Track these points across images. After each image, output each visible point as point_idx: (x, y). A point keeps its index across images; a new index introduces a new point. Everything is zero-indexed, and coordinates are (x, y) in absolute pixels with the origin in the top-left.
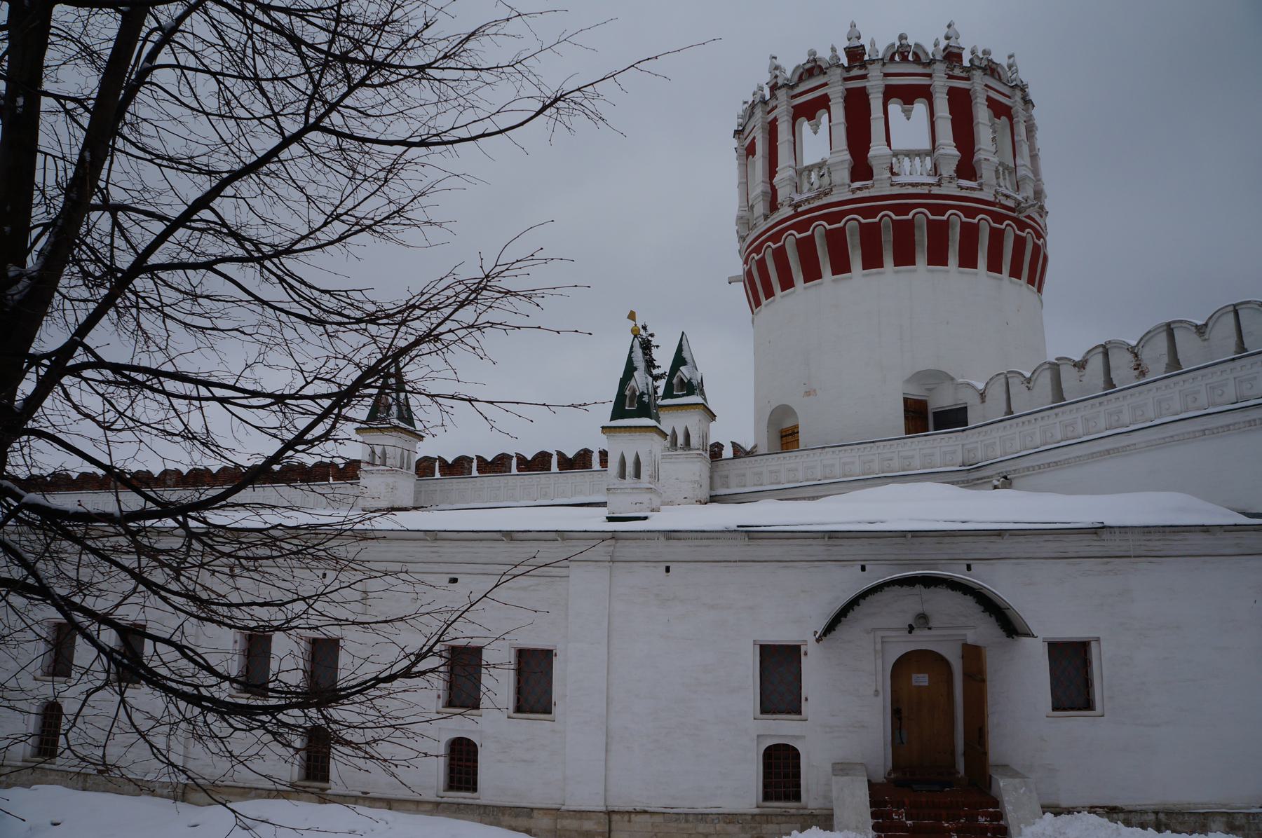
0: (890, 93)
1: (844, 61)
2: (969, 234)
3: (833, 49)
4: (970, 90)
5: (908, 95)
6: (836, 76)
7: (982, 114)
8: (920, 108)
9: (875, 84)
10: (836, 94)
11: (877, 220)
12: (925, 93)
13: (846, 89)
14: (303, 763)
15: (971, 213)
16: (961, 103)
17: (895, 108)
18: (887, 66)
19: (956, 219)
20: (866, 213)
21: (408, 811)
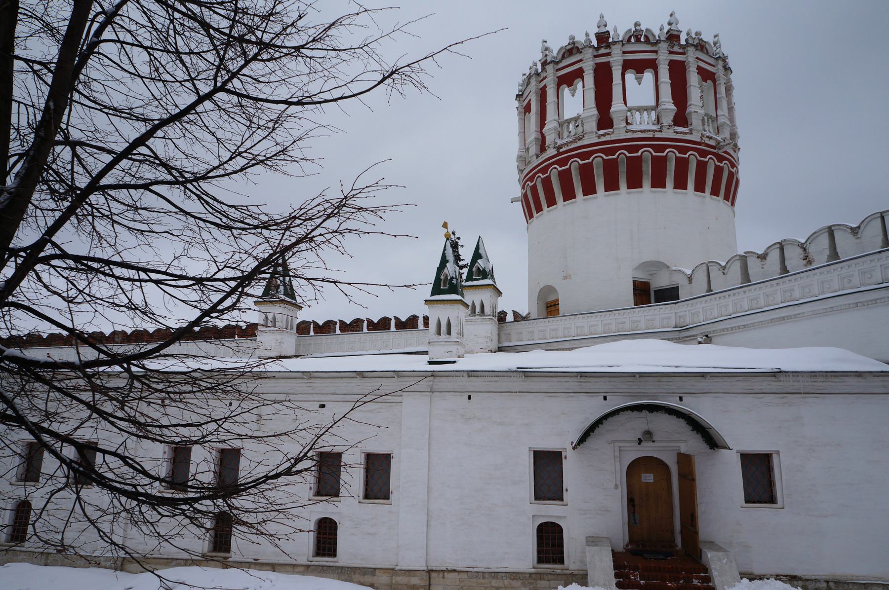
1: (595, 43)
2: (682, 166)
3: (587, 35)
5: (639, 67)
6: (588, 54)
9: (616, 59)
12: (652, 65)
13: (595, 64)
14: (212, 539)
18: (626, 46)
19: (672, 155)
21: (287, 572)
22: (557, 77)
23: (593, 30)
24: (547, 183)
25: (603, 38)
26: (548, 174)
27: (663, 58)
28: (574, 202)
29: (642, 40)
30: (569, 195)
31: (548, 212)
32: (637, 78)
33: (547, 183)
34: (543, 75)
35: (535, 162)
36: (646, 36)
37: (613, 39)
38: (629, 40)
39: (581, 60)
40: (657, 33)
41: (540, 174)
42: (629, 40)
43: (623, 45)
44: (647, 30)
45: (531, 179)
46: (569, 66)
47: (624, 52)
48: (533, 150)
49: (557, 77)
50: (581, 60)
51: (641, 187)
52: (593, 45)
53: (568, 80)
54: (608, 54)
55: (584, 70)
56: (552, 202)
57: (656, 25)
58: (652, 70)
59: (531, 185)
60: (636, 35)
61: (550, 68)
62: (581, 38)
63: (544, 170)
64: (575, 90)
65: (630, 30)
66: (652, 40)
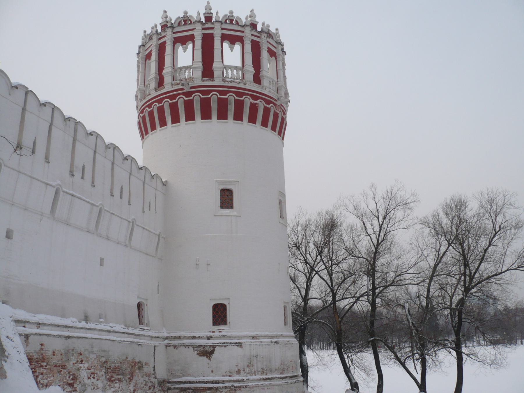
0: (224, 38)
1: (203, 20)
2: (254, 109)
3: (199, 14)
4: (260, 42)
6: (199, 27)
7: (265, 54)
8: (237, 47)
9: (217, 33)
10: (198, 34)
11: (209, 96)
12: (240, 40)
15: (255, 98)
16: (256, 47)
17: (226, 45)
18: (223, 24)
19: (248, 101)
20: (203, 92)
22: (174, 38)
23: (203, 11)
24: (161, 110)
26: (162, 104)
28: (178, 126)
29: (234, 22)
30: (176, 120)
31: (160, 130)
32: (230, 47)
33: (161, 110)
34: (163, 34)
35: (154, 94)
36: (236, 21)
37: (215, 19)
38: (226, 22)
39: (193, 29)
40: (244, 20)
41: (156, 103)
42: (226, 22)
43: (222, 23)
44: (238, 17)
45: (149, 106)
46: (183, 31)
47: (222, 29)
48: (153, 85)
49: (174, 38)
50: (193, 29)
51: (227, 119)
52: (202, 21)
53: (183, 40)
54: (212, 28)
55: (195, 37)
56: (163, 123)
58: (239, 43)
59: (149, 110)
61: (169, 31)
62: (193, 14)
63: (159, 101)
64: (187, 48)
65: (226, 15)
66: (240, 24)
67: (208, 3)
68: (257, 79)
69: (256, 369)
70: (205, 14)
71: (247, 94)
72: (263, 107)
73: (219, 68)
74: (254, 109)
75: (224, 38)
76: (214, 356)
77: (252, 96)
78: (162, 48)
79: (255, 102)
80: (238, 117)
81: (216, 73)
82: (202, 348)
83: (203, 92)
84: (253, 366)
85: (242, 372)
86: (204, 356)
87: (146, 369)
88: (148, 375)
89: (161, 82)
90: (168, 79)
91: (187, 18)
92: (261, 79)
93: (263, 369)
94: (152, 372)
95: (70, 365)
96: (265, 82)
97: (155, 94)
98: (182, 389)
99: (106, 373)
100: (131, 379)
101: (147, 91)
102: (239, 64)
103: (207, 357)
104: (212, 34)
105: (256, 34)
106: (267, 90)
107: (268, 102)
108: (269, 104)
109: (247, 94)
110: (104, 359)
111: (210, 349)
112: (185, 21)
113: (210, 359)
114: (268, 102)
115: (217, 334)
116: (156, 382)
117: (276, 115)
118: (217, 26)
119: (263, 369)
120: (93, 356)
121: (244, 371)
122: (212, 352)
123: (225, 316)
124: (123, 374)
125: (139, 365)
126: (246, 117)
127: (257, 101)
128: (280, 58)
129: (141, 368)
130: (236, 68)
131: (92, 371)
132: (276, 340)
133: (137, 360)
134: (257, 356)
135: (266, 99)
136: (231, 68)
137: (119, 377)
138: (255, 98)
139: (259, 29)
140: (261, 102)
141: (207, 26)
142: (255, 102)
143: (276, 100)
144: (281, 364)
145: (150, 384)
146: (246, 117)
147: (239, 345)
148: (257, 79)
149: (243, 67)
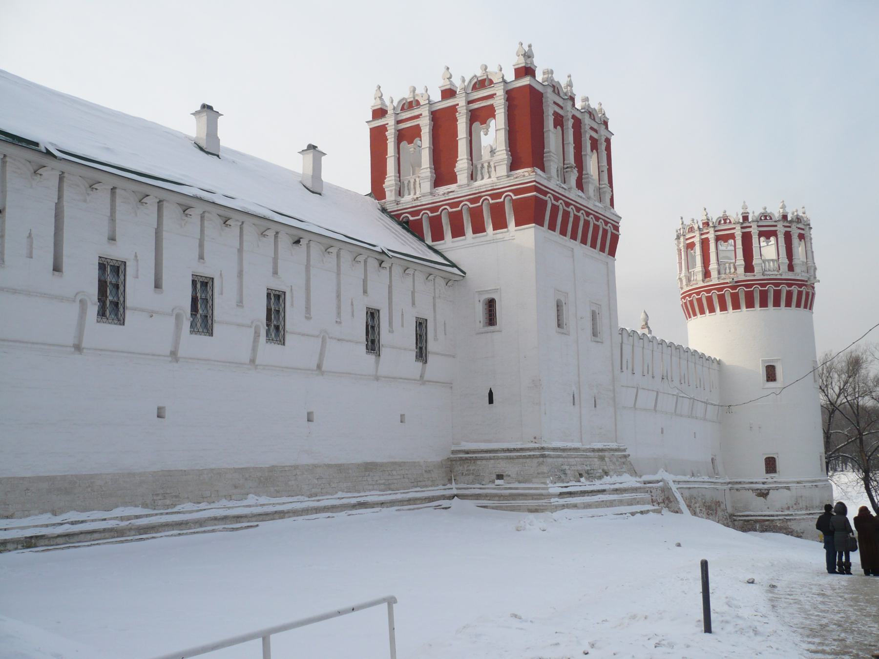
0: (761, 234)
1: (741, 221)
3: (737, 215)
5: (767, 234)
6: (738, 227)
7: (795, 241)
8: (773, 240)
9: (754, 231)
10: (738, 233)
11: (752, 289)
12: (774, 234)
13: (742, 232)
15: (790, 285)
16: (788, 237)
19: (784, 289)
20: (747, 286)
23: (741, 211)
25: (745, 218)
27: (781, 229)
57: (776, 212)
60: (765, 216)
67: (744, 202)
68: (791, 268)
69: (801, 506)
70: (742, 214)
71: (783, 283)
72: (797, 291)
73: (759, 264)
74: (789, 294)
75: (761, 234)
76: (769, 497)
77: (787, 284)
78: (705, 243)
79: (790, 289)
80: (777, 304)
81: (756, 269)
82: (759, 490)
83: (747, 286)
84: (799, 504)
85: (791, 509)
86: (761, 496)
87: (723, 506)
88: (723, 511)
89: (707, 274)
90: (714, 274)
91: (726, 218)
92: (794, 266)
93: (806, 506)
94: (725, 508)
95: (692, 505)
96: (797, 269)
97: (702, 284)
98: (745, 521)
99: (706, 509)
100: (716, 513)
101: (691, 277)
102: (775, 257)
103: (764, 497)
104: (750, 232)
105: (788, 224)
106: (800, 275)
107: (800, 286)
108: (801, 288)
109: (783, 283)
110: (704, 501)
111: (766, 492)
112: (725, 220)
113: (766, 499)
114: (800, 286)
115: (770, 480)
116: (728, 516)
117: (807, 294)
118: (754, 225)
119: (806, 506)
120: (700, 499)
121: (792, 507)
122: (767, 494)
123: (775, 467)
124: (712, 510)
125: (718, 503)
126: (783, 303)
127: (791, 287)
128: (807, 239)
129: (719, 506)
130: (773, 260)
131: (700, 508)
132: (815, 484)
133: (717, 501)
134: (801, 497)
135: (799, 284)
136: (769, 261)
137: (711, 512)
138: (790, 285)
139: (789, 219)
140: (795, 287)
141: (745, 225)
142: (790, 289)
143: (807, 281)
144: (821, 503)
145: (725, 517)
146: (783, 303)
147: (788, 488)
148: (791, 268)
149: (778, 259)
